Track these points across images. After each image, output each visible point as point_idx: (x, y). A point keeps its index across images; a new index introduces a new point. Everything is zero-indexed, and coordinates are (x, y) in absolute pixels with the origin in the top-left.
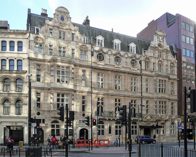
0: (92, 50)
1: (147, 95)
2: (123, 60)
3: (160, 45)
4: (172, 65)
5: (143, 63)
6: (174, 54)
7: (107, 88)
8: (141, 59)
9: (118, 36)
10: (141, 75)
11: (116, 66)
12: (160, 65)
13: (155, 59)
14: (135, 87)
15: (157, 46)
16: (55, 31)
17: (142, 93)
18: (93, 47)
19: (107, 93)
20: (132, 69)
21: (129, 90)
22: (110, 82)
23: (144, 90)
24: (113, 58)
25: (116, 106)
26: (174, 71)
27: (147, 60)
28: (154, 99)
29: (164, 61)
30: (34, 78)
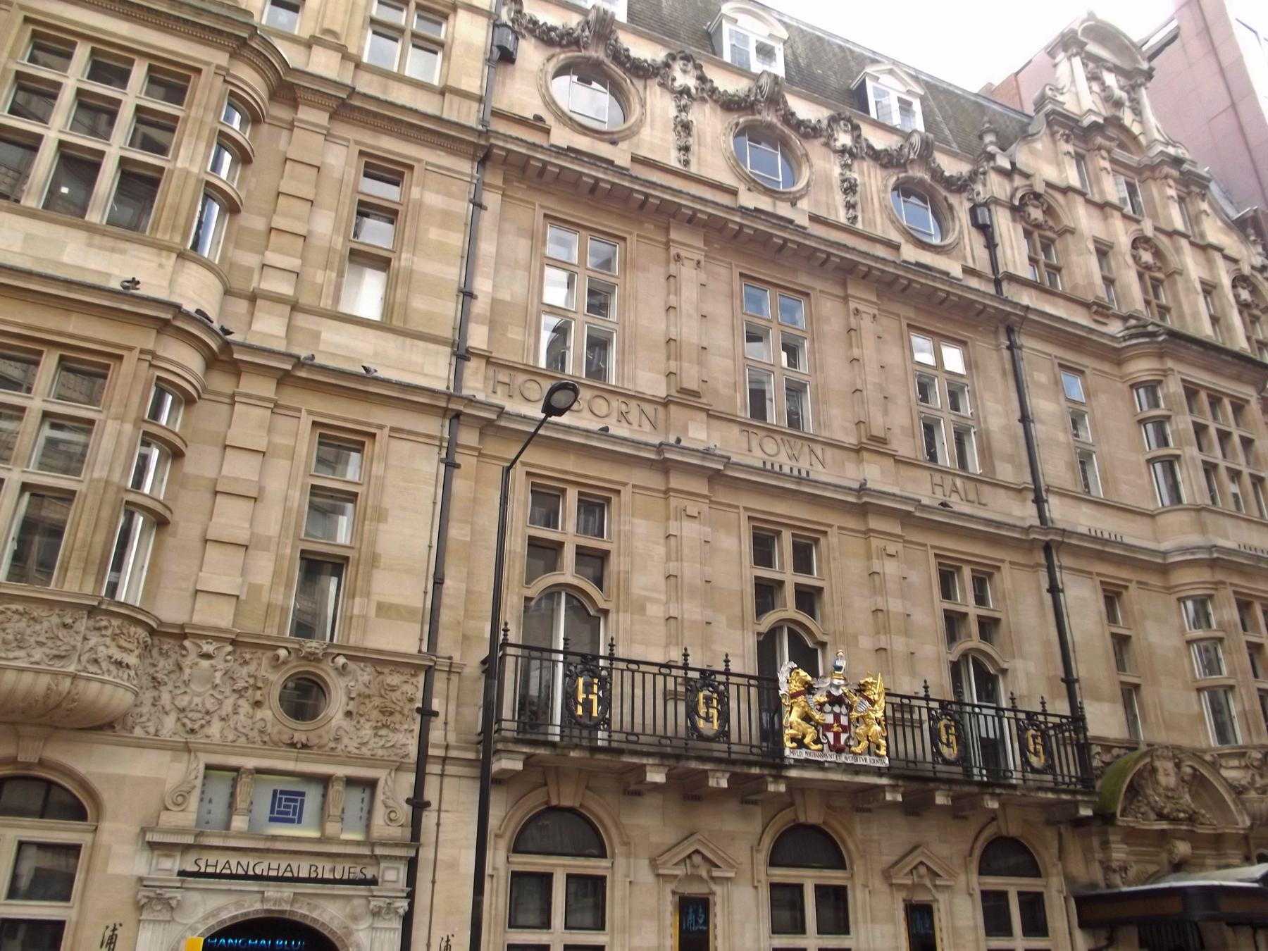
7: (652, 383)
8: (982, 191)
10: (1009, 325)
12: (1157, 276)
14: (960, 438)
17: (1039, 501)
25: (770, 619)
27: (1036, 214)
28: (1183, 577)
29: (1178, 250)
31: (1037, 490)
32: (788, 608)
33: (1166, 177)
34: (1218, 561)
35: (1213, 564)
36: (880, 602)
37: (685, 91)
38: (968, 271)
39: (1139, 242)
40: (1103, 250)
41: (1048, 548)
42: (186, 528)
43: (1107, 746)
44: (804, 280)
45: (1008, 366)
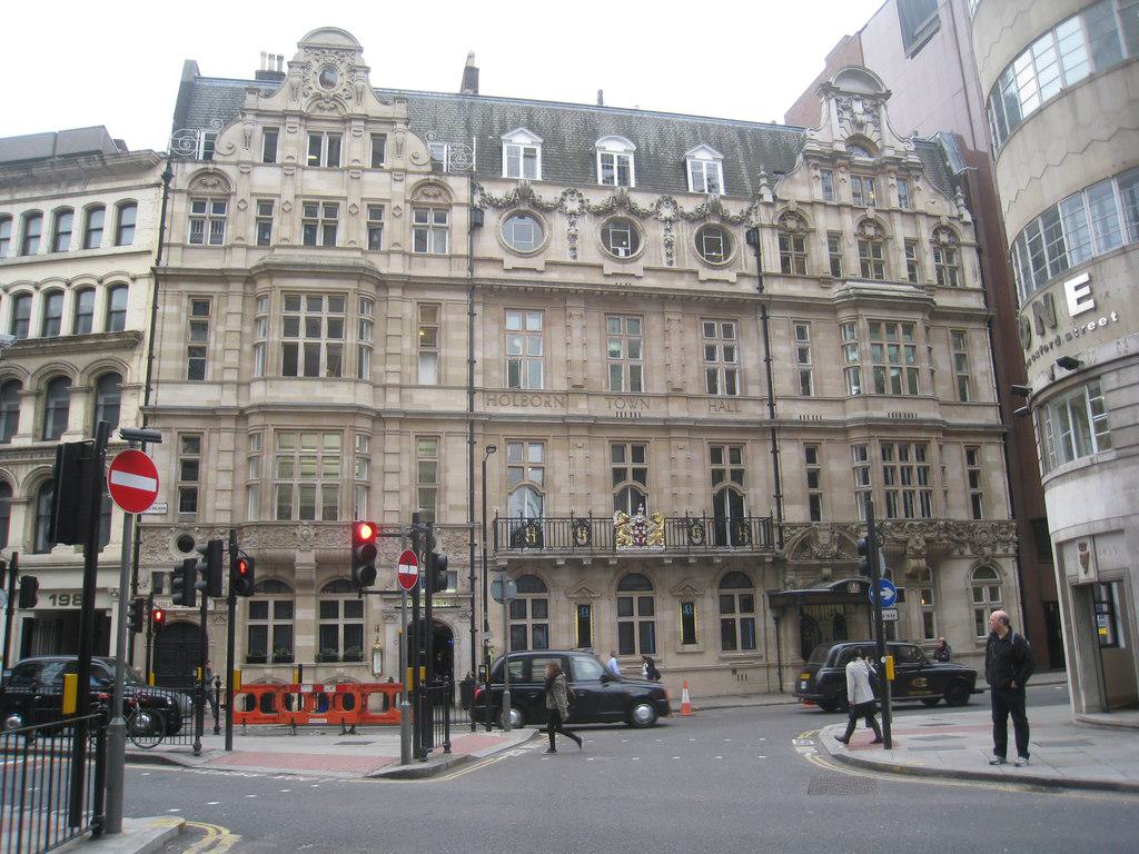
0: (477, 199)
1: (803, 413)
2: (652, 234)
3: (858, 142)
4: (944, 238)
5: (770, 242)
6: (949, 184)
7: (560, 385)
9: (626, 123)
10: (761, 306)
11: (610, 268)
13: (840, 214)
15: (841, 147)
16: (293, 137)
17: (771, 405)
18: (482, 184)
19: (563, 418)
20: (705, 274)
21: (692, 390)
22: (577, 354)
23: (785, 383)
24: (590, 229)
26: (960, 268)
27: (792, 224)
29: (892, 221)
30: (172, 359)
31: (771, 398)
32: (630, 481)
33: (889, 172)
34: (871, 426)
35: (870, 427)
36: (674, 471)
37: (573, 214)
38: (740, 276)
39: (863, 223)
40: (834, 239)
41: (773, 431)
42: (377, 487)
43: (794, 526)
44: (641, 307)
45: (761, 329)
